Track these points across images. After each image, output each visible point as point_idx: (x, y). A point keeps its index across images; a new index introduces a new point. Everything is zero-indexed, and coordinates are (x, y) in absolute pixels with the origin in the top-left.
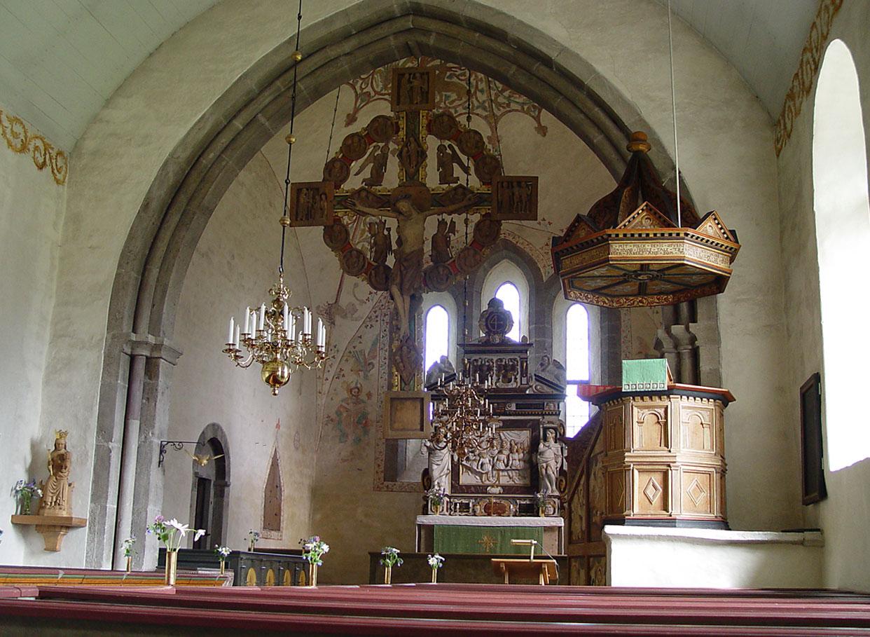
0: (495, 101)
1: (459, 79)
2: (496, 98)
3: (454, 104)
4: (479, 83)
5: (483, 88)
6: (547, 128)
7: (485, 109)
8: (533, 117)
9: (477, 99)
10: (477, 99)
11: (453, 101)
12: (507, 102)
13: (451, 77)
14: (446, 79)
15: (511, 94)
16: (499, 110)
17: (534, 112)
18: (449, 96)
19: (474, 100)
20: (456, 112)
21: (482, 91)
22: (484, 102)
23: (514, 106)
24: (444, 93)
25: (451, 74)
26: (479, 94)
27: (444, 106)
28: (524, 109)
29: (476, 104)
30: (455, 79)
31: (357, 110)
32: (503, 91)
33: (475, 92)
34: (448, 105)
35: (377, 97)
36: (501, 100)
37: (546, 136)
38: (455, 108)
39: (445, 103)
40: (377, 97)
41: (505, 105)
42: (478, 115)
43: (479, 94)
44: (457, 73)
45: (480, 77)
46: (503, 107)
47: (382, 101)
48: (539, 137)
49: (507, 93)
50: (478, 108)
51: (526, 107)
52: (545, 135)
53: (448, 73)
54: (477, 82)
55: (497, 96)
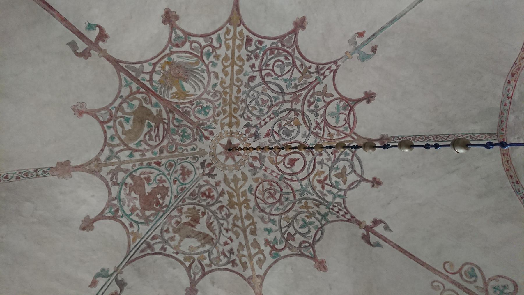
0: (119, 169)
1: (146, 134)
2: (122, 170)
3: (118, 127)
4: (140, 153)
5: (134, 156)
6: (92, 230)
7: (109, 158)
8: (103, 211)
9: (122, 150)
10: (122, 150)
11: (122, 126)
12: (119, 182)
13: (149, 126)
14: (147, 121)
15: (128, 185)
16: (108, 174)
17: (110, 212)
18: (128, 122)
19: (121, 147)
20: (109, 127)
21: (131, 155)
22: (118, 158)
23: (115, 190)
24: (132, 117)
25: (151, 126)
26: (127, 152)
27: (118, 116)
28: (114, 200)
29: (116, 149)
30: (146, 129)
31: (173, 28)
32: (131, 176)
33: (130, 149)
34: (119, 120)
35: (167, 51)
36: (121, 176)
37: (82, 231)
38: (114, 127)
39: (121, 117)
40: (167, 51)
41: (114, 180)
42: (102, 150)
43: (127, 152)
44: (152, 133)
45: (146, 154)
46: (112, 179)
47: (156, 55)
48: (78, 224)
49: (129, 181)
50: (111, 151)
51: (115, 202)
52: (84, 229)
53: (153, 124)
54: (140, 151)
55: (126, 171)
